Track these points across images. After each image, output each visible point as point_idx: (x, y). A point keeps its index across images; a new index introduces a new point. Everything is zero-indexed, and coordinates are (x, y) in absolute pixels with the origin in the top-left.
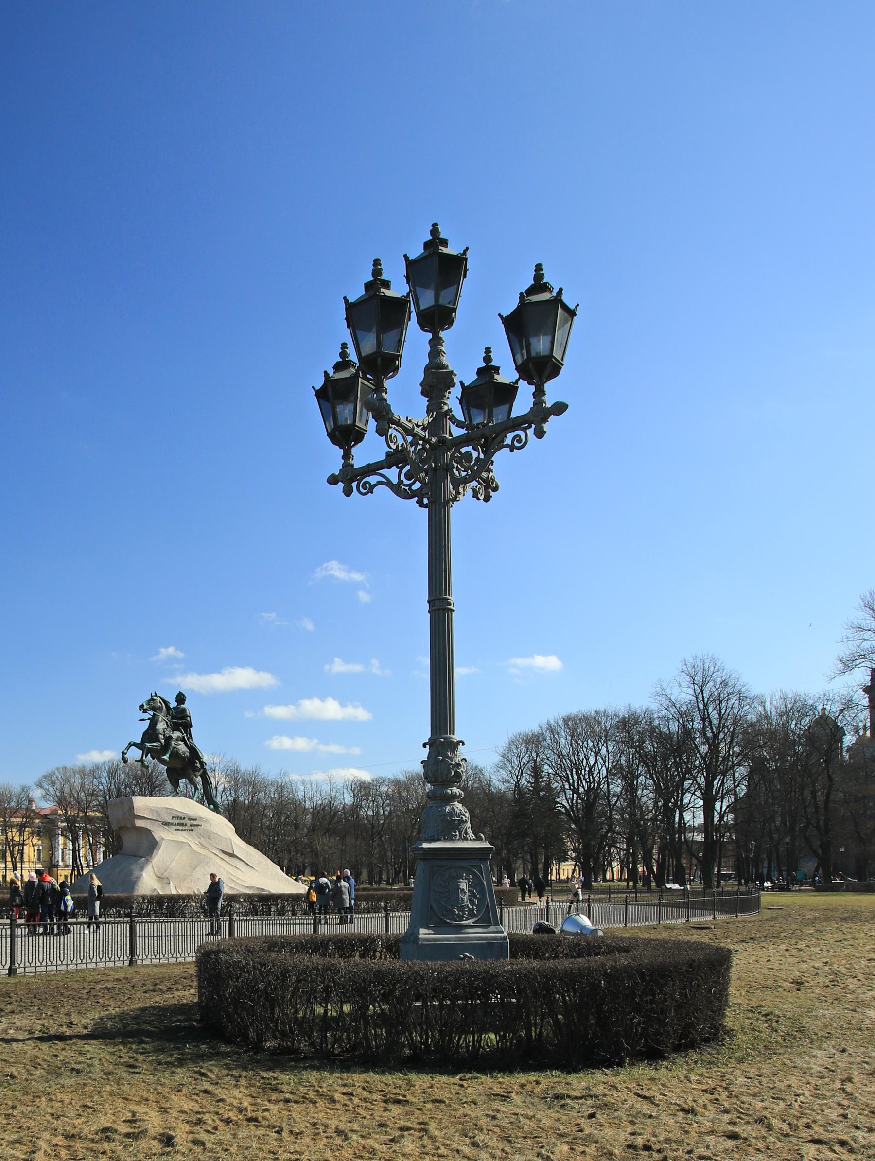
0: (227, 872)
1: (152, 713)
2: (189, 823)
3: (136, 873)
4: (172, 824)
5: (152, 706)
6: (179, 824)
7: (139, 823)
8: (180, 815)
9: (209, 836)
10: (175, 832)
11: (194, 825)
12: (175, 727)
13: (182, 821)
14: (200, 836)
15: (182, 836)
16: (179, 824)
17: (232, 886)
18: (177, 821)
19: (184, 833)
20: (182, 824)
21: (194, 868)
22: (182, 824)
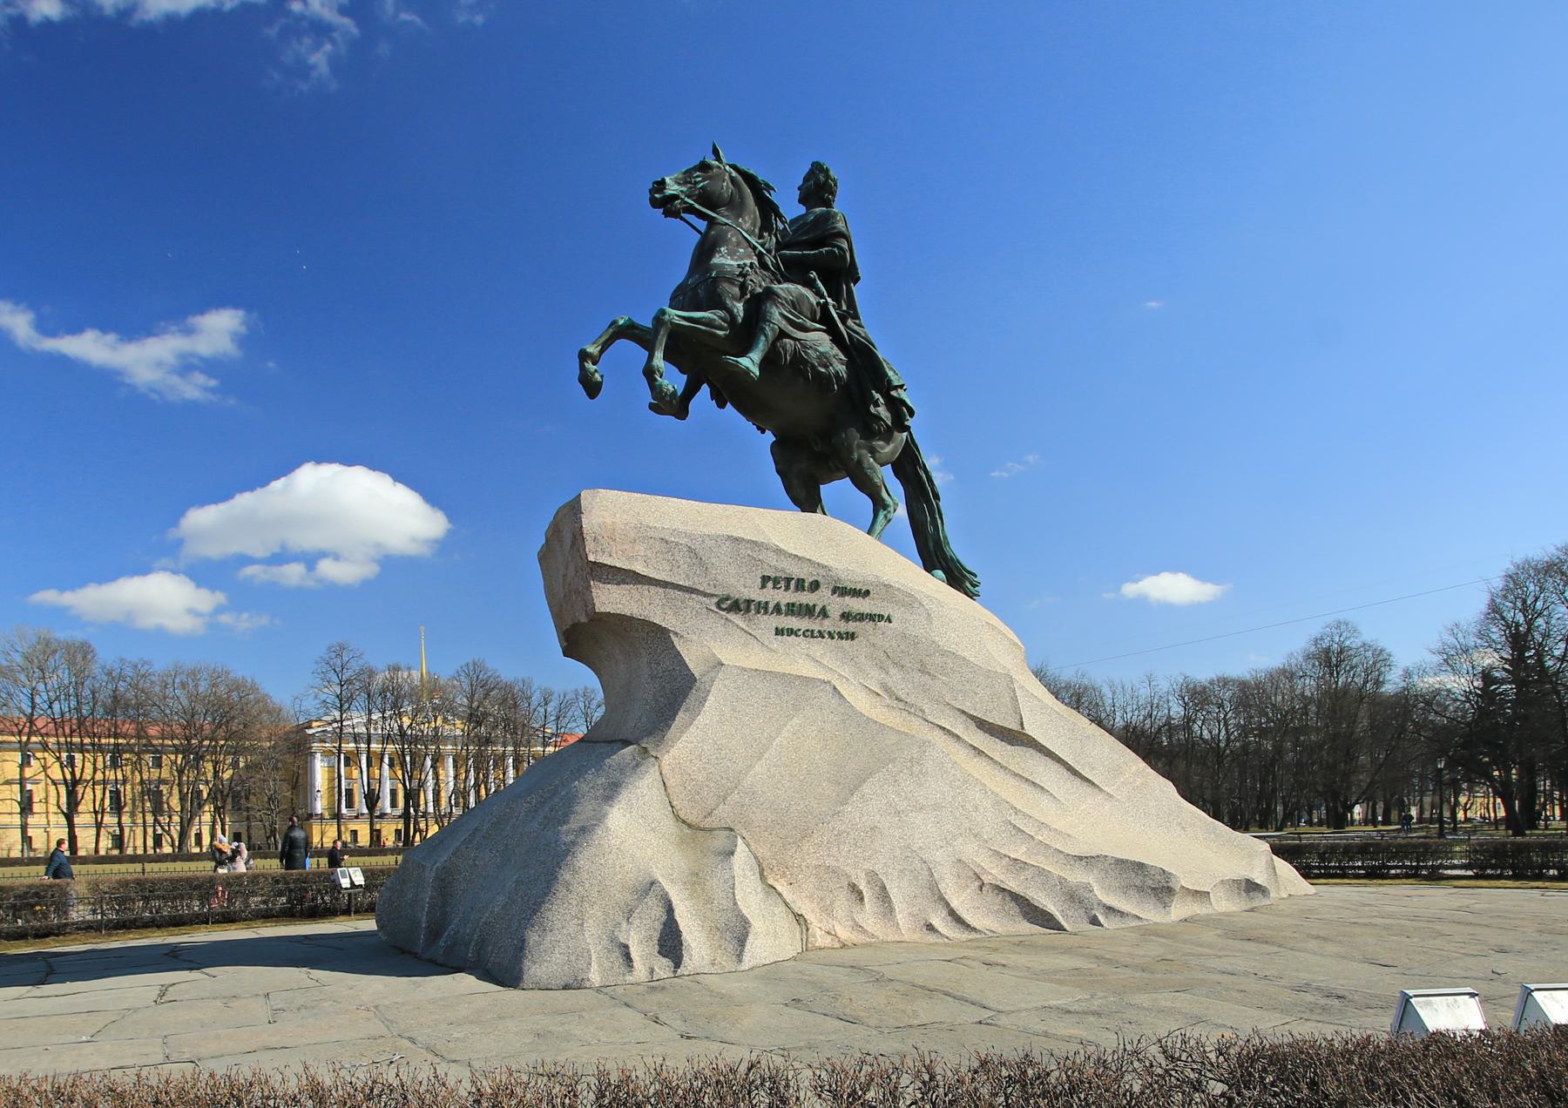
0: (999, 802)
1: (702, 225)
2: (837, 605)
3: (584, 810)
4: (763, 608)
5: (704, 199)
6: (792, 609)
7: (609, 599)
8: (797, 571)
9: (925, 661)
10: (777, 643)
11: (861, 617)
12: (795, 271)
13: (805, 598)
14: (887, 660)
15: (804, 659)
16: (792, 609)
17: (1019, 852)
18: (785, 597)
19: (818, 647)
20: (808, 611)
21: (850, 787)
22: (808, 611)
